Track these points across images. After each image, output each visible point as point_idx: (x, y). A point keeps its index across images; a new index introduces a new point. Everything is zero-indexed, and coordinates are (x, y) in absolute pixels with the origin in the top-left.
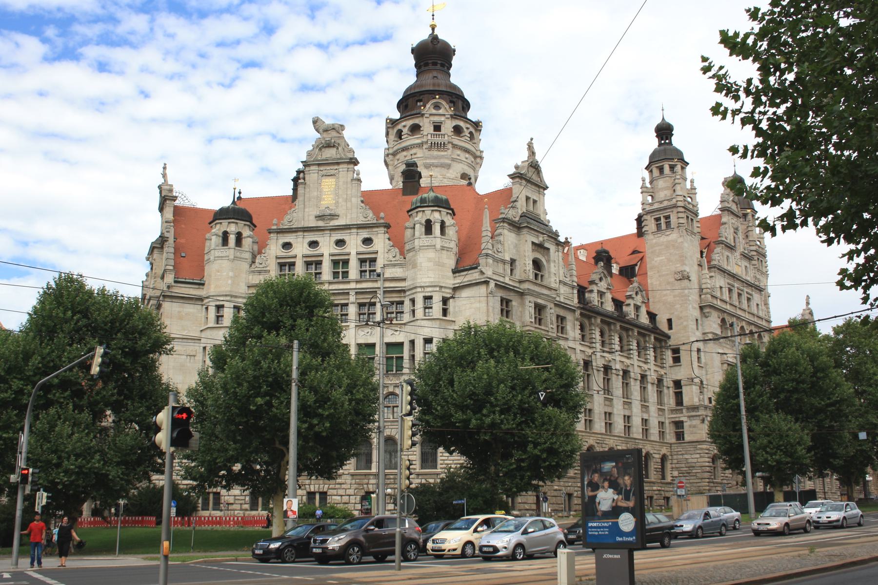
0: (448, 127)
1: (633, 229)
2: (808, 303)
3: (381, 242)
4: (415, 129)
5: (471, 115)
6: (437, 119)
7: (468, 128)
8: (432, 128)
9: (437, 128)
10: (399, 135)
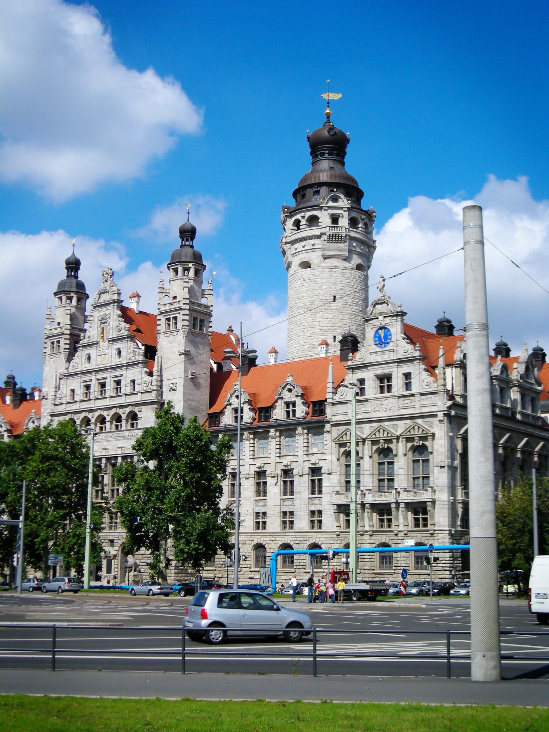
4: (313, 221)
5: (365, 204)
7: (363, 219)
8: (330, 220)
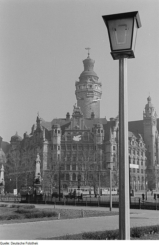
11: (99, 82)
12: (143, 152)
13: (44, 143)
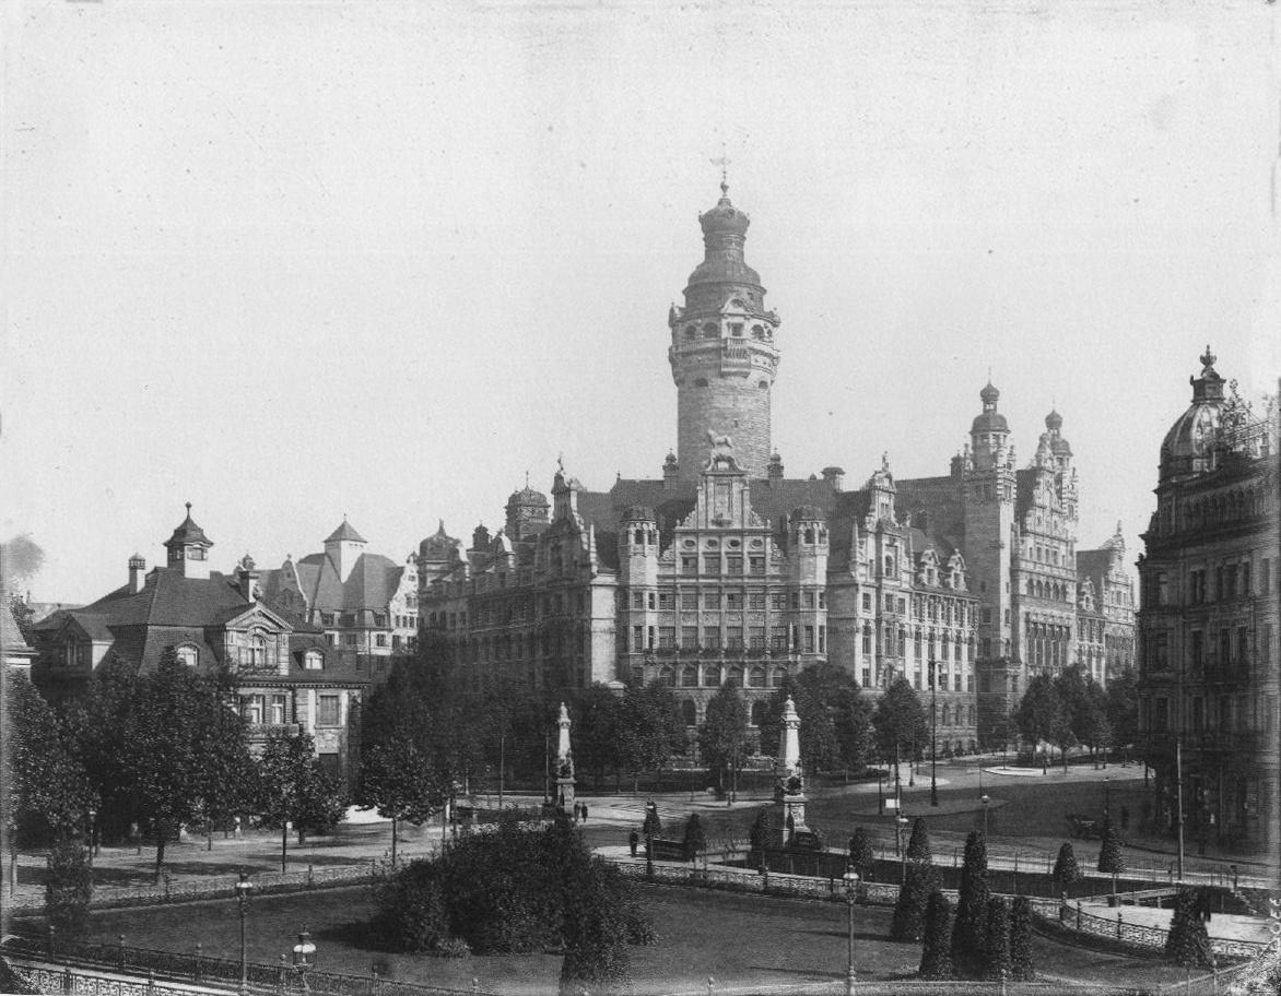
0: (748, 326)
1: (946, 472)
2: (1119, 530)
3: (769, 547)
6: (737, 320)
9: (737, 329)
10: (691, 332)
11: (767, 308)
12: (962, 610)
13: (594, 581)
